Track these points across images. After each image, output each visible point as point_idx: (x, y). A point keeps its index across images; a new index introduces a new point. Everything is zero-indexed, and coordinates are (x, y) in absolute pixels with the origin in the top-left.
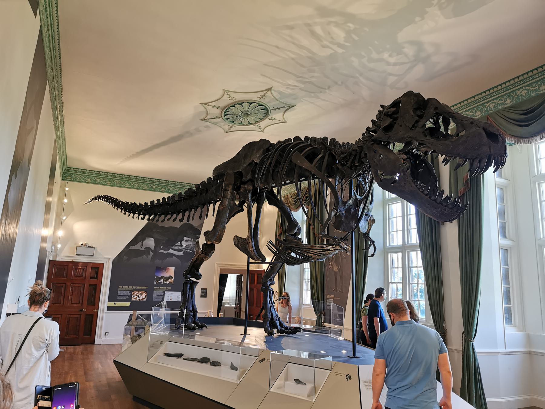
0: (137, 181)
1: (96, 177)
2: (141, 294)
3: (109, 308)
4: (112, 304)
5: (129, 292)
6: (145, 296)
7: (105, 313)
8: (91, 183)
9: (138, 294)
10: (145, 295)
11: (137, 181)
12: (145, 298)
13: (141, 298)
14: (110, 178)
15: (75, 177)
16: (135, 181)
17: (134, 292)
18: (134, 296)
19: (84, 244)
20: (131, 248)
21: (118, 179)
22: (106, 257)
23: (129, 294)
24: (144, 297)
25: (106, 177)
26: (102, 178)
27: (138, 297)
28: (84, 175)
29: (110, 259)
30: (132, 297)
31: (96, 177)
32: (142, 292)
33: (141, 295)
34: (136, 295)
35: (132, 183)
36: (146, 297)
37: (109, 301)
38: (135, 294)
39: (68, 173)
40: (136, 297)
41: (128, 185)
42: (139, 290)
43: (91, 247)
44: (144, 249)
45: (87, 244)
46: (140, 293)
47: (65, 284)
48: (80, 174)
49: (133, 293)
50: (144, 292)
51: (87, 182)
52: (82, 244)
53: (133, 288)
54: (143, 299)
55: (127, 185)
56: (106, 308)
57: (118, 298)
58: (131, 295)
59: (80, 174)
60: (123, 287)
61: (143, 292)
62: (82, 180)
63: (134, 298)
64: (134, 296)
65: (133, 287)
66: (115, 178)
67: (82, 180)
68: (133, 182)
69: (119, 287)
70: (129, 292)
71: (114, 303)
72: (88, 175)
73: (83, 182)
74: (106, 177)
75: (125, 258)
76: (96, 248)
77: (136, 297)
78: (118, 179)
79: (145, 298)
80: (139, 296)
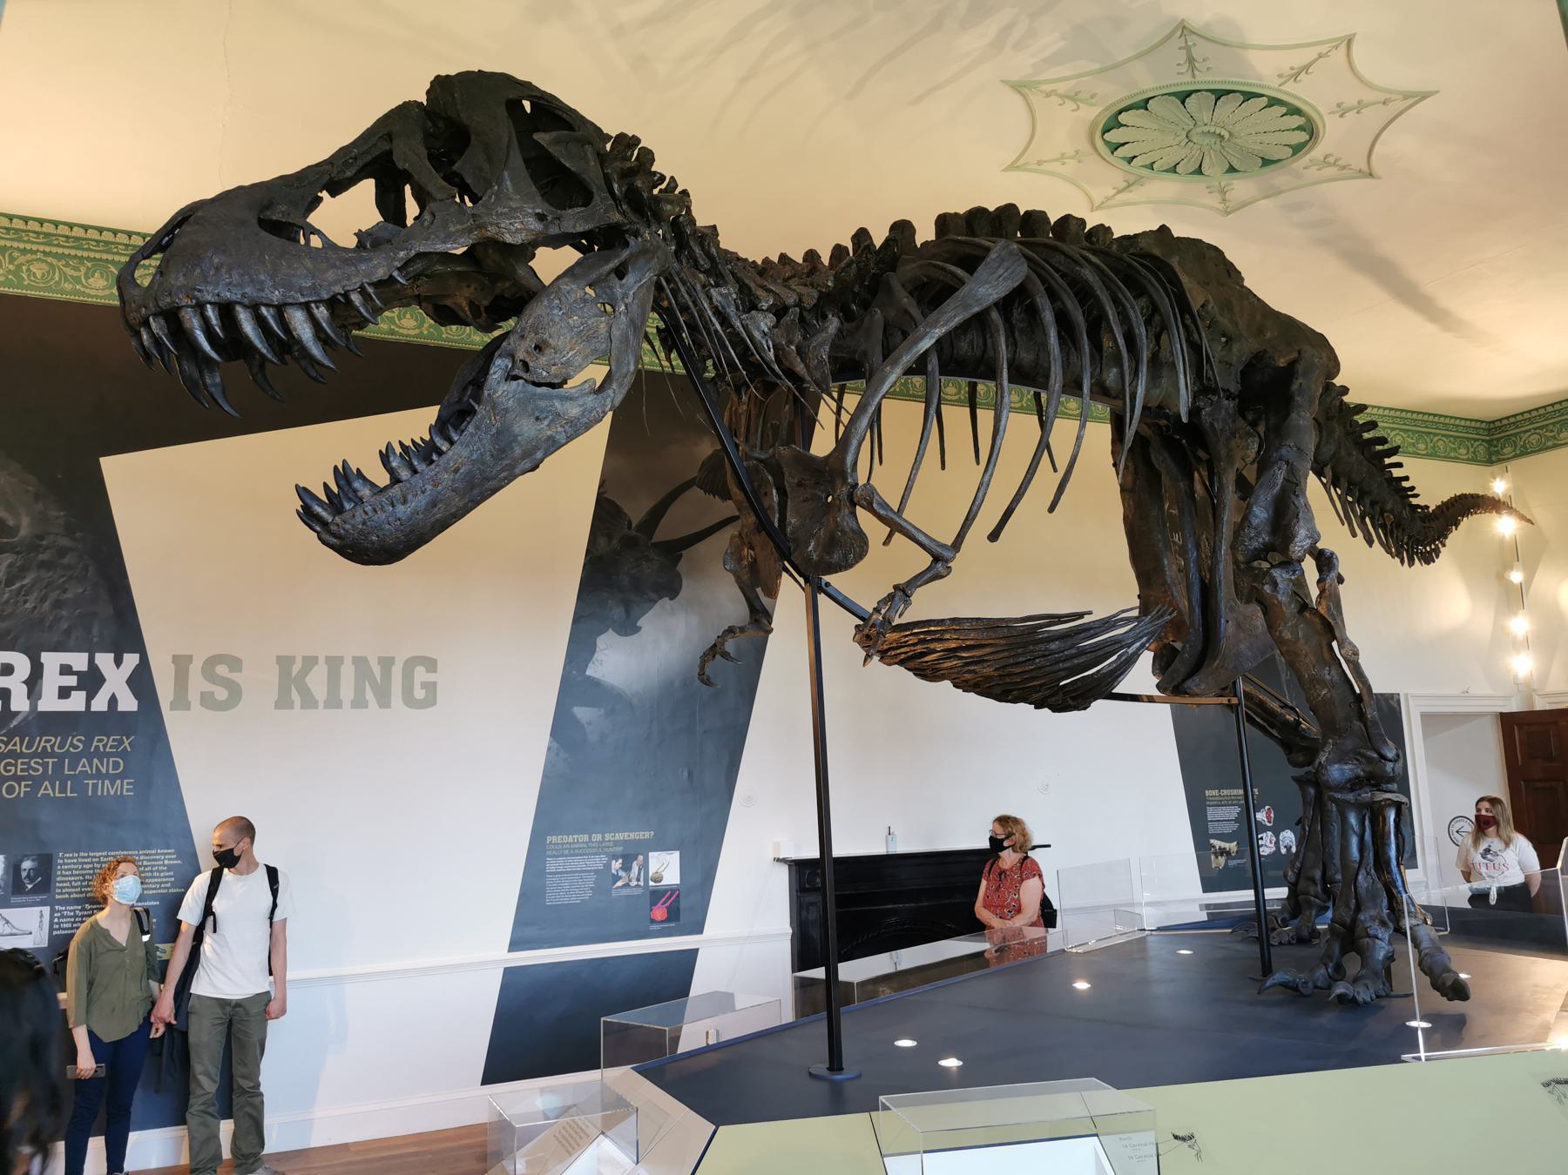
15: (1524, 442)
28: (1547, 425)
48: (1535, 426)
51: (1562, 445)
59: (1535, 426)
73: (1548, 448)
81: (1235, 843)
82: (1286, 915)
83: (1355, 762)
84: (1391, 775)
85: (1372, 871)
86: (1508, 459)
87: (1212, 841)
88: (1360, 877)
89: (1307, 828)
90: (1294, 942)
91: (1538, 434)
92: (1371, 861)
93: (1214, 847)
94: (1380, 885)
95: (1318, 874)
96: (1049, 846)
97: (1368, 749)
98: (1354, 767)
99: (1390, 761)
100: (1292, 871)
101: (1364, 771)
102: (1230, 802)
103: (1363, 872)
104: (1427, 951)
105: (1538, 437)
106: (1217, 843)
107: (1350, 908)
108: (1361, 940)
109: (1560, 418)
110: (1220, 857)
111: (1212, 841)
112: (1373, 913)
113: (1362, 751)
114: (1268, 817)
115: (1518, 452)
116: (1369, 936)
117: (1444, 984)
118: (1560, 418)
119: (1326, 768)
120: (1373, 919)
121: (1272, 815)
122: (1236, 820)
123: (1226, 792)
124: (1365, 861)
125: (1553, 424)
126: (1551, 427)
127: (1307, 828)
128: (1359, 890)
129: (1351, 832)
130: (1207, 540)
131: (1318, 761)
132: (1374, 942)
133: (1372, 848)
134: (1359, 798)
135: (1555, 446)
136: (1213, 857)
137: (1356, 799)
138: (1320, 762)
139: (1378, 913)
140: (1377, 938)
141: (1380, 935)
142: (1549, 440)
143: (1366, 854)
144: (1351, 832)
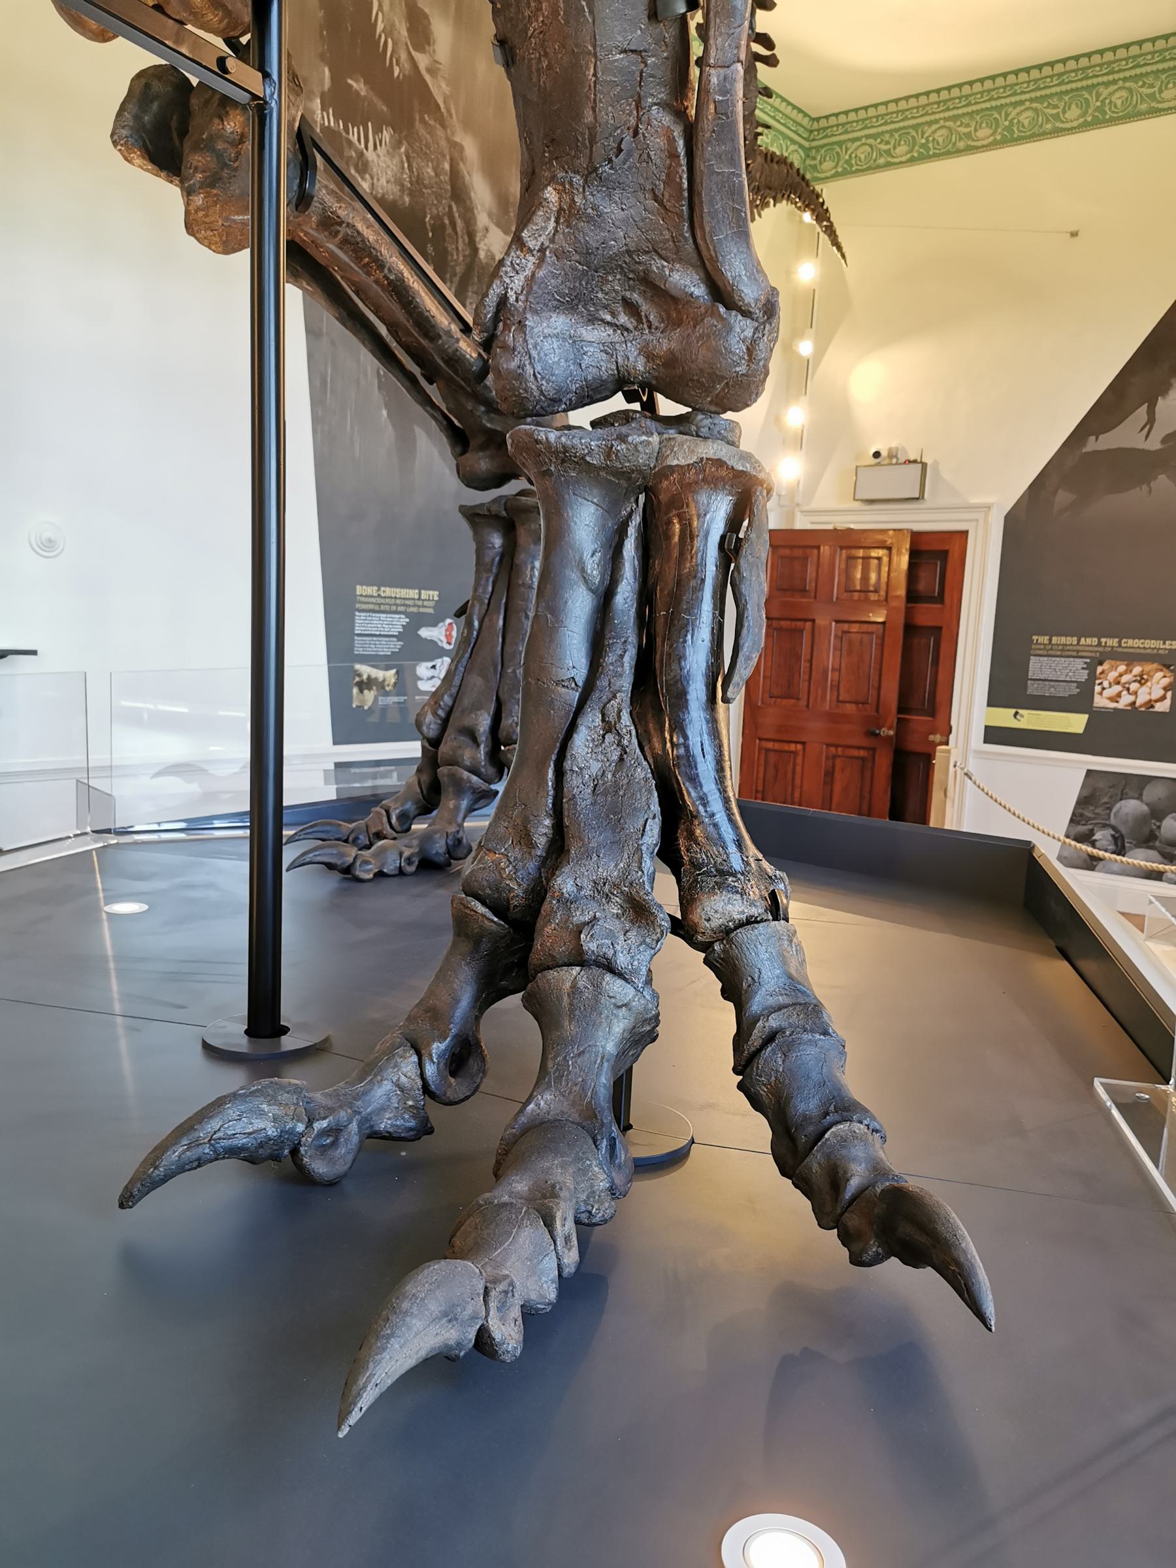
0: (1122, 75)
1: (930, 124)
2: (1141, 676)
3: (994, 735)
4: (1004, 717)
5: (1079, 663)
6: (1166, 689)
7: (976, 752)
8: (912, 161)
9: (1124, 679)
10: (1166, 681)
11: (1122, 75)
12: (1163, 698)
13: (1141, 699)
14: (988, 105)
16: (1111, 77)
17: (1106, 666)
18: (1106, 684)
19: (884, 453)
20: (1093, 445)
21: (1023, 97)
22: (974, 500)
23: (1083, 676)
24: (1157, 693)
25: (969, 109)
26: (954, 118)
27: (1128, 689)
28: (883, 133)
29: (989, 508)
30: (1098, 689)
31: (930, 124)
32: (1149, 667)
33: (1141, 680)
34: (1118, 683)
35: (1098, 95)
36: (1169, 694)
37: (994, 700)
38: (1113, 675)
39: (825, 145)
40: (1117, 689)
41: (1074, 113)
42: (1131, 659)
43: (915, 461)
44: (1163, 441)
45: (897, 449)
46: (1137, 670)
47: (814, 621)
48: (867, 132)
49: (1100, 669)
50: (1157, 670)
52: (877, 455)
53: (1099, 644)
54: (1150, 704)
55: (1069, 115)
56: (978, 734)
57: (1033, 689)
58: (1092, 677)
59: (867, 132)
60: (1055, 640)
61: (1155, 666)
62: (875, 160)
63: (1107, 693)
64: (1106, 684)
65: (1099, 644)
66: (1008, 100)
67: (875, 160)
68: (1101, 89)
69: (1035, 638)
70: (1079, 663)
71: (1014, 711)
72: (897, 126)
74: (969, 109)
75: (1063, 497)
76: (936, 463)
77: (1117, 689)
78: (1023, 97)
79: (1163, 698)
80: (1134, 686)
81: (394, 671)
82: (409, 806)
83: (623, 319)
84: (742, 369)
85: (626, 719)
86: (827, 178)
87: (358, 666)
88: (581, 742)
89: (476, 624)
90: (411, 869)
91: (871, 146)
92: (626, 683)
93: (360, 675)
94: (642, 772)
95: (483, 723)
96: (34, 653)
97: (677, 257)
98: (617, 337)
99: (746, 314)
100: (435, 714)
101: (649, 356)
102: (394, 608)
103: (591, 720)
104: (774, 1022)
105: (868, 149)
106: (365, 670)
107: (531, 845)
108: (552, 974)
109: (901, 124)
110: (366, 692)
111: (358, 666)
112: (609, 868)
113: (656, 264)
114: (448, 637)
115: (840, 170)
116: (579, 959)
117: (836, 1177)
118: (901, 124)
119: (521, 325)
120: (602, 891)
121: (454, 634)
122: (399, 637)
123: (388, 591)
124: (602, 682)
125: (891, 132)
126: (887, 137)
127: (476, 624)
128: (573, 783)
129: (574, 575)
130: (408, 157)
131: (496, 290)
132: (597, 986)
133: (632, 638)
134: (622, 447)
135: (888, 165)
136: (355, 690)
137: (609, 452)
138: (503, 301)
139: (627, 871)
140: (609, 967)
141: (622, 961)
142: (881, 155)
143: (611, 658)
144: (574, 575)
